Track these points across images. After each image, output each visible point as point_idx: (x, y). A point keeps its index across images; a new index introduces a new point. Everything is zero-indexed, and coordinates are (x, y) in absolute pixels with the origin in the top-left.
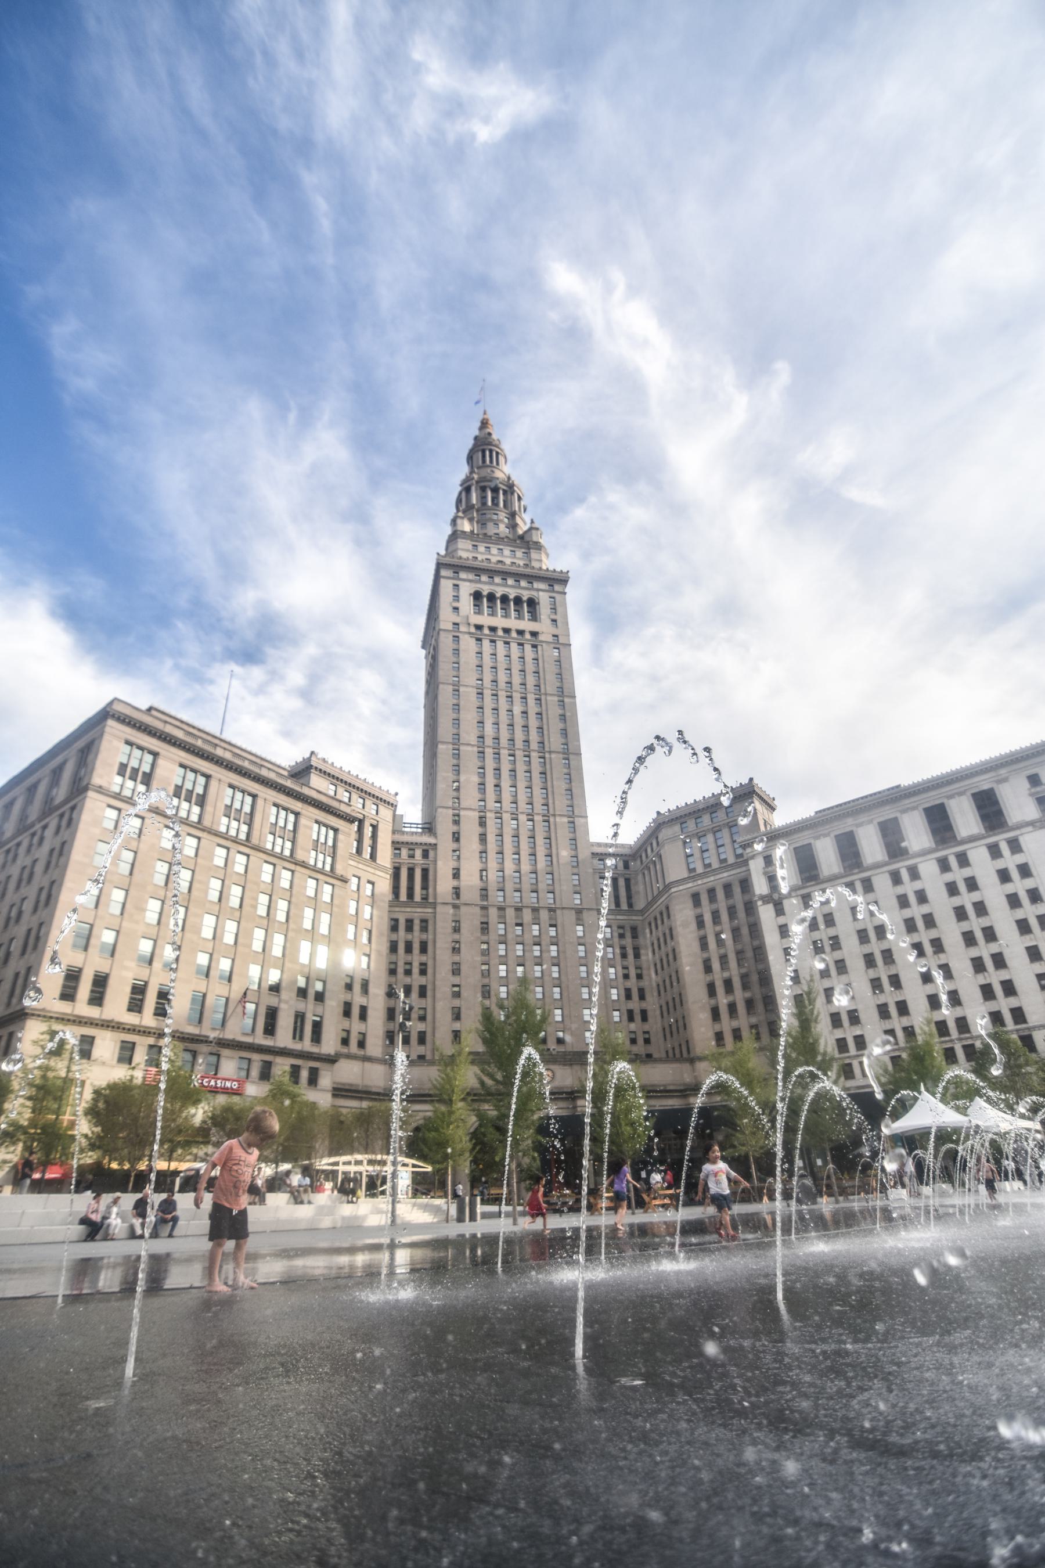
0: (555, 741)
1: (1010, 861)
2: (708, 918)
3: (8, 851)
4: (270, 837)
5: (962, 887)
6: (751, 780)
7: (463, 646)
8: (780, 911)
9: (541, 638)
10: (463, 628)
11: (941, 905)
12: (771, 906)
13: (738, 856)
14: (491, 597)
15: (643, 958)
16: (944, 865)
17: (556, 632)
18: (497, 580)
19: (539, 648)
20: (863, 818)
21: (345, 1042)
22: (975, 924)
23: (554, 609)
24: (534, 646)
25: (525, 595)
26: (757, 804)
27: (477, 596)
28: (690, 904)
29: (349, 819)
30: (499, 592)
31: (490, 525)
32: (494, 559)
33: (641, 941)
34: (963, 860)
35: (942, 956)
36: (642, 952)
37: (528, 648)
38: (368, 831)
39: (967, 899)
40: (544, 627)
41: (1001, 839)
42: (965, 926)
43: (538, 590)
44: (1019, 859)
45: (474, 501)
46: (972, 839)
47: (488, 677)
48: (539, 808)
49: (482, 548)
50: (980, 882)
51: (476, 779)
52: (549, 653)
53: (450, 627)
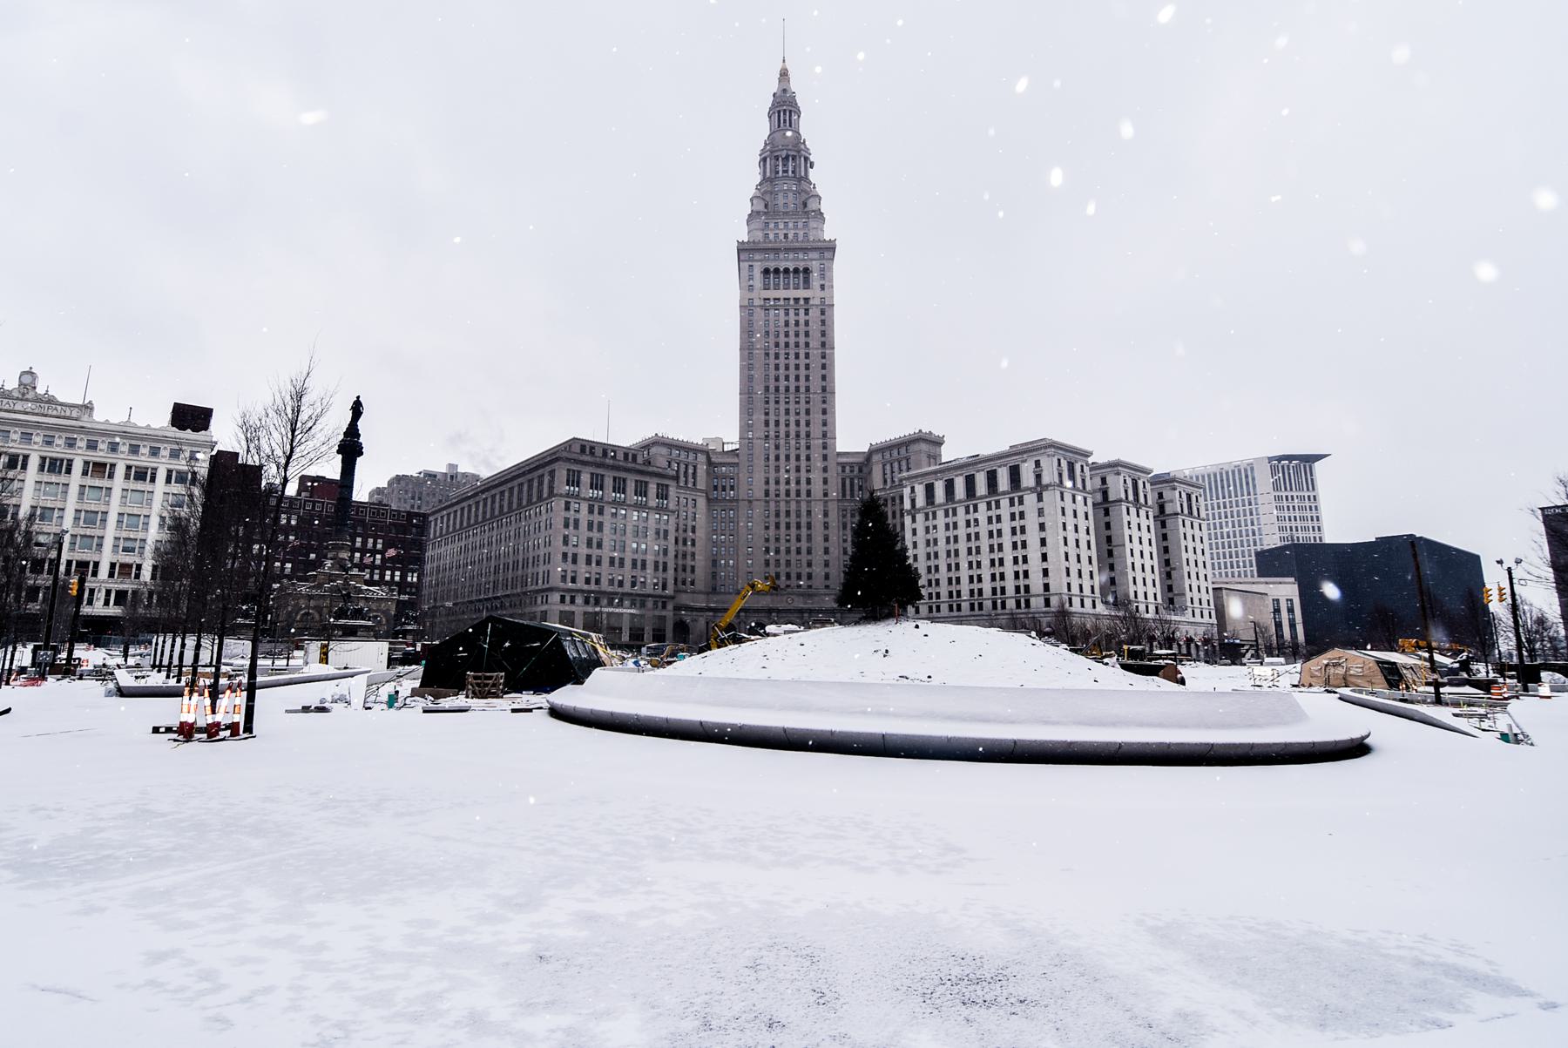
0: (816, 384)
7: (756, 317)
10: (757, 302)
11: (983, 529)
14: (777, 271)
17: (822, 294)
18: (781, 256)
21: (684, 583)
23: (822, 276)
26: (924, 447)
27: (766, 272)
29: (676, 478)
38: (691, 471)
40: (814, 293)
41: (1015, 495)
47: (772, 339)
48: (803, 435)
51: (763, 417)
52: (814, 313)
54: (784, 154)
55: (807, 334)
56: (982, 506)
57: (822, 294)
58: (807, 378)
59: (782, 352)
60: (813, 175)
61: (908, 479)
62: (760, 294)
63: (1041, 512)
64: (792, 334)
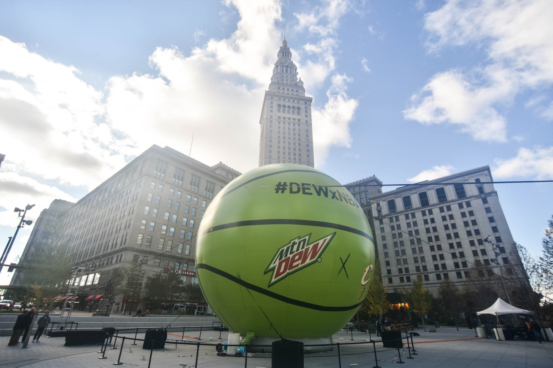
1: (466, 210)
3: (120, 194)
4: (205, 192)
5: (448, 218)
8: (381, 223)
9: (301, 121)
10: (273, 117)
11: (439, 224)
12: (378, 221)
13: (367, 202)
14: (284, 106)
16: (442, 210)
17: (306, 119)
18: (287, 100)
20: (414, 191)
22: (451, 231)
24: (299, 125)
27: (279, 106)
31: (285, 80)
32: (286, 93)
34: (449, 208)
35: (439, 242)
37: (296, 125)
39: (449, 222)
42: (448, 232)
44: (470, 209)
45: (279, 71)
46: (453, 201)
47: (282, 135)
49: (281, 89)
50: (455, 216)
53: (269, 117)
54: (286, 65)
55: (299, 135)
56: (436, 211)
57: (306, 119)
58: (300, 155)
60: (298, 77)
61: (373, 199)
62: (276, 114)
63: (488, 210)
64: (292, 134)
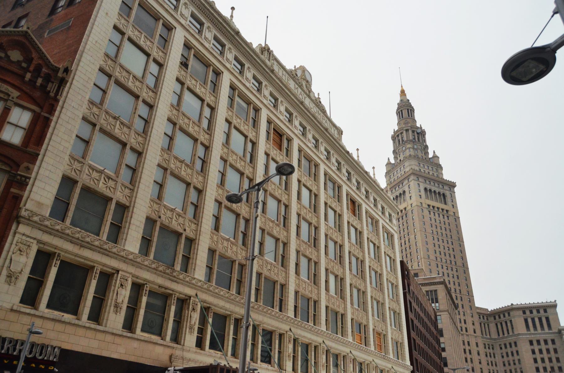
2: (537, 351)
6: (555, 301)
10: (424, 205)
15: (497, 358)
19: (449, 218)
24: (448, 217)
25: (442, 191)
27: (426, 189)
28: (528, 343)
30: (433, 189)
33: (495, 351)
36: (496, 355)
43: (446, 190)
45: (411, 138)
52: (452, 219)
53: (420, 204)
59: (440, 238)
